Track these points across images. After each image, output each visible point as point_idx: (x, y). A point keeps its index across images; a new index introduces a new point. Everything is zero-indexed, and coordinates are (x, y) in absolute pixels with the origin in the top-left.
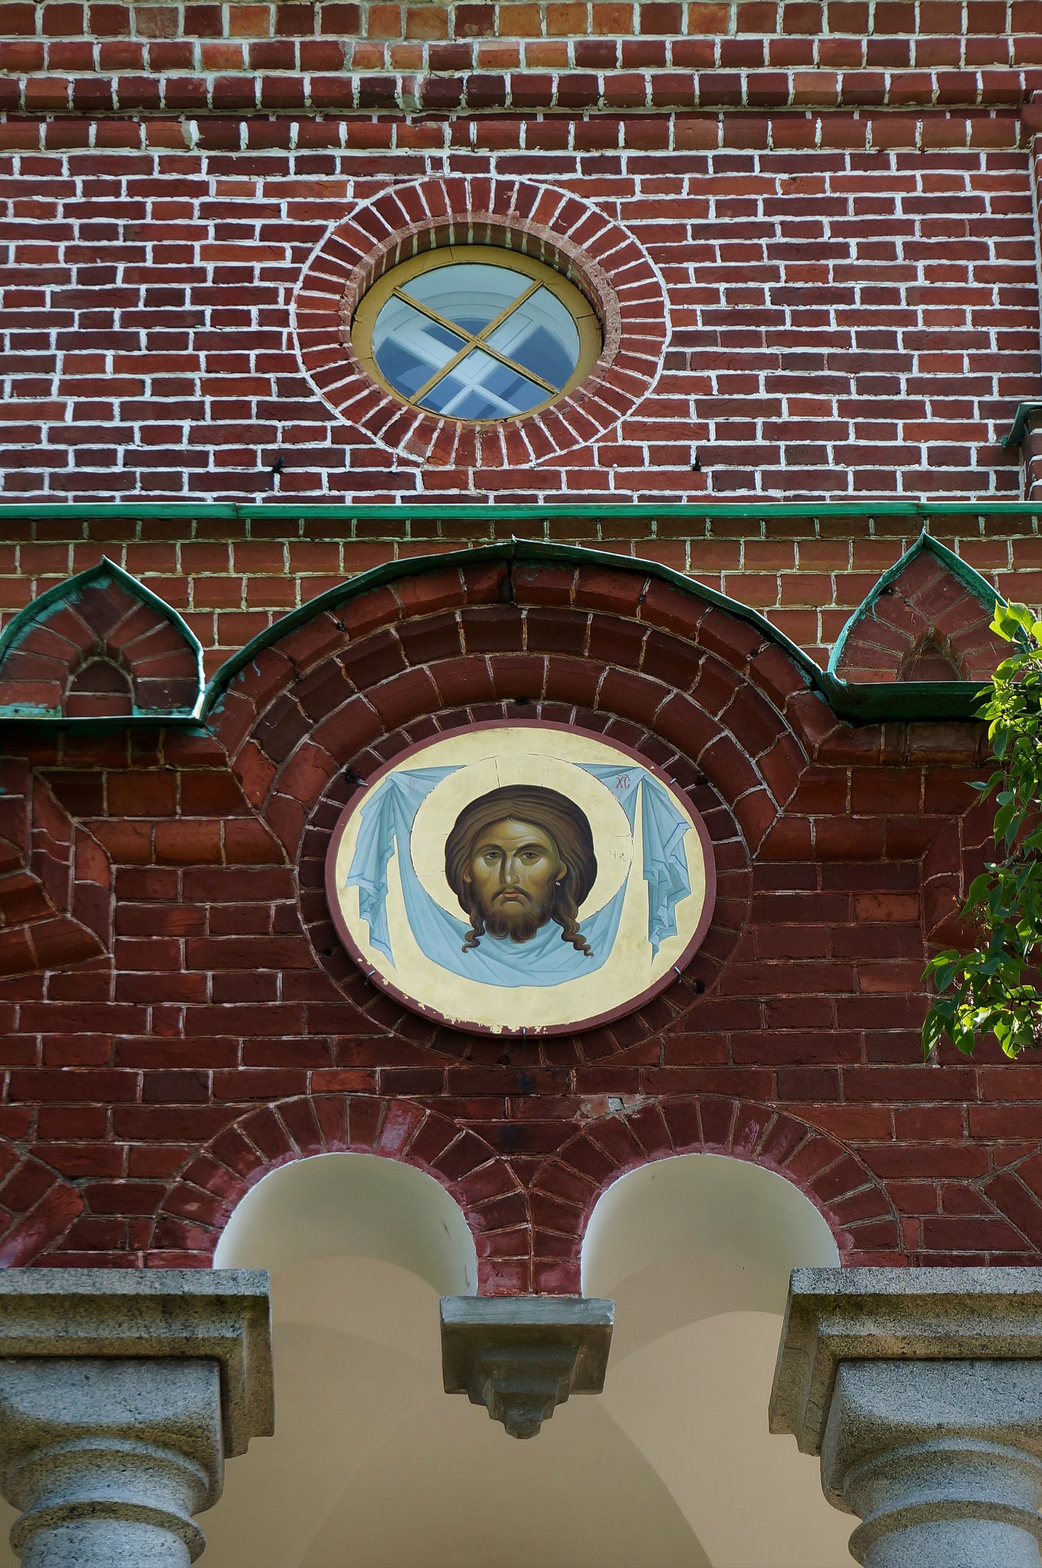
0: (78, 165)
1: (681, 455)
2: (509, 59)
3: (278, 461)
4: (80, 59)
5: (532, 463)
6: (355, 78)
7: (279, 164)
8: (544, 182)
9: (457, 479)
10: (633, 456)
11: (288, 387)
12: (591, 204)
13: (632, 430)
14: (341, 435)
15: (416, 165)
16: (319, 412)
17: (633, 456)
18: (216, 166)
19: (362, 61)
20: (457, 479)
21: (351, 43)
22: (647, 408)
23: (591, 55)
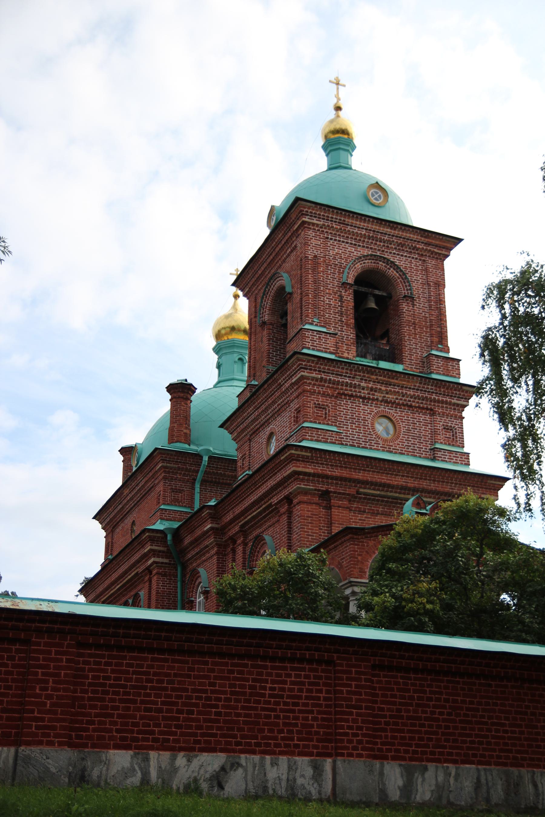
0: (351, 402)
1: (403, 445)
2: (389, 398)
3: (369, 440)
4: (351, 391)
5: (391, 444)
6: (376, 397)
7: (368, 405)
8: (391, 411)
9: (384, 445)
10: (399, 444)
11: (370, 432)
12: (395, 414)
13: (400, 442)
14: (375, 438)
15: (380, 407)
16: (372, 435)
17: (399, 444)
18: (363, 404)
19: (377, 396)
20: (384, 445)
21: (376, 394)
22: (401, 439)
23: (397, 399)
